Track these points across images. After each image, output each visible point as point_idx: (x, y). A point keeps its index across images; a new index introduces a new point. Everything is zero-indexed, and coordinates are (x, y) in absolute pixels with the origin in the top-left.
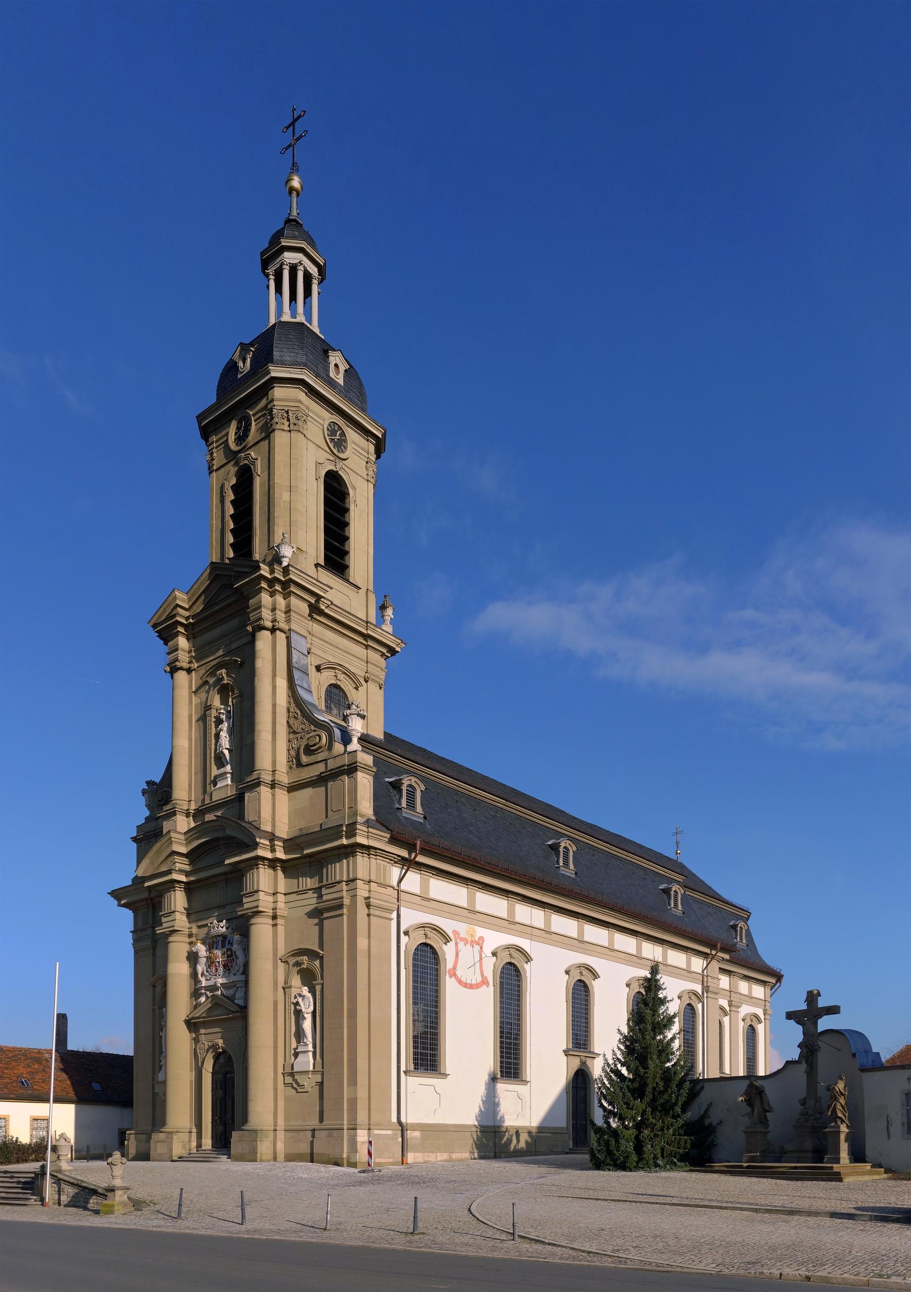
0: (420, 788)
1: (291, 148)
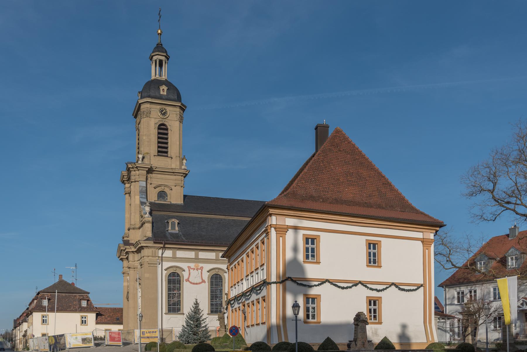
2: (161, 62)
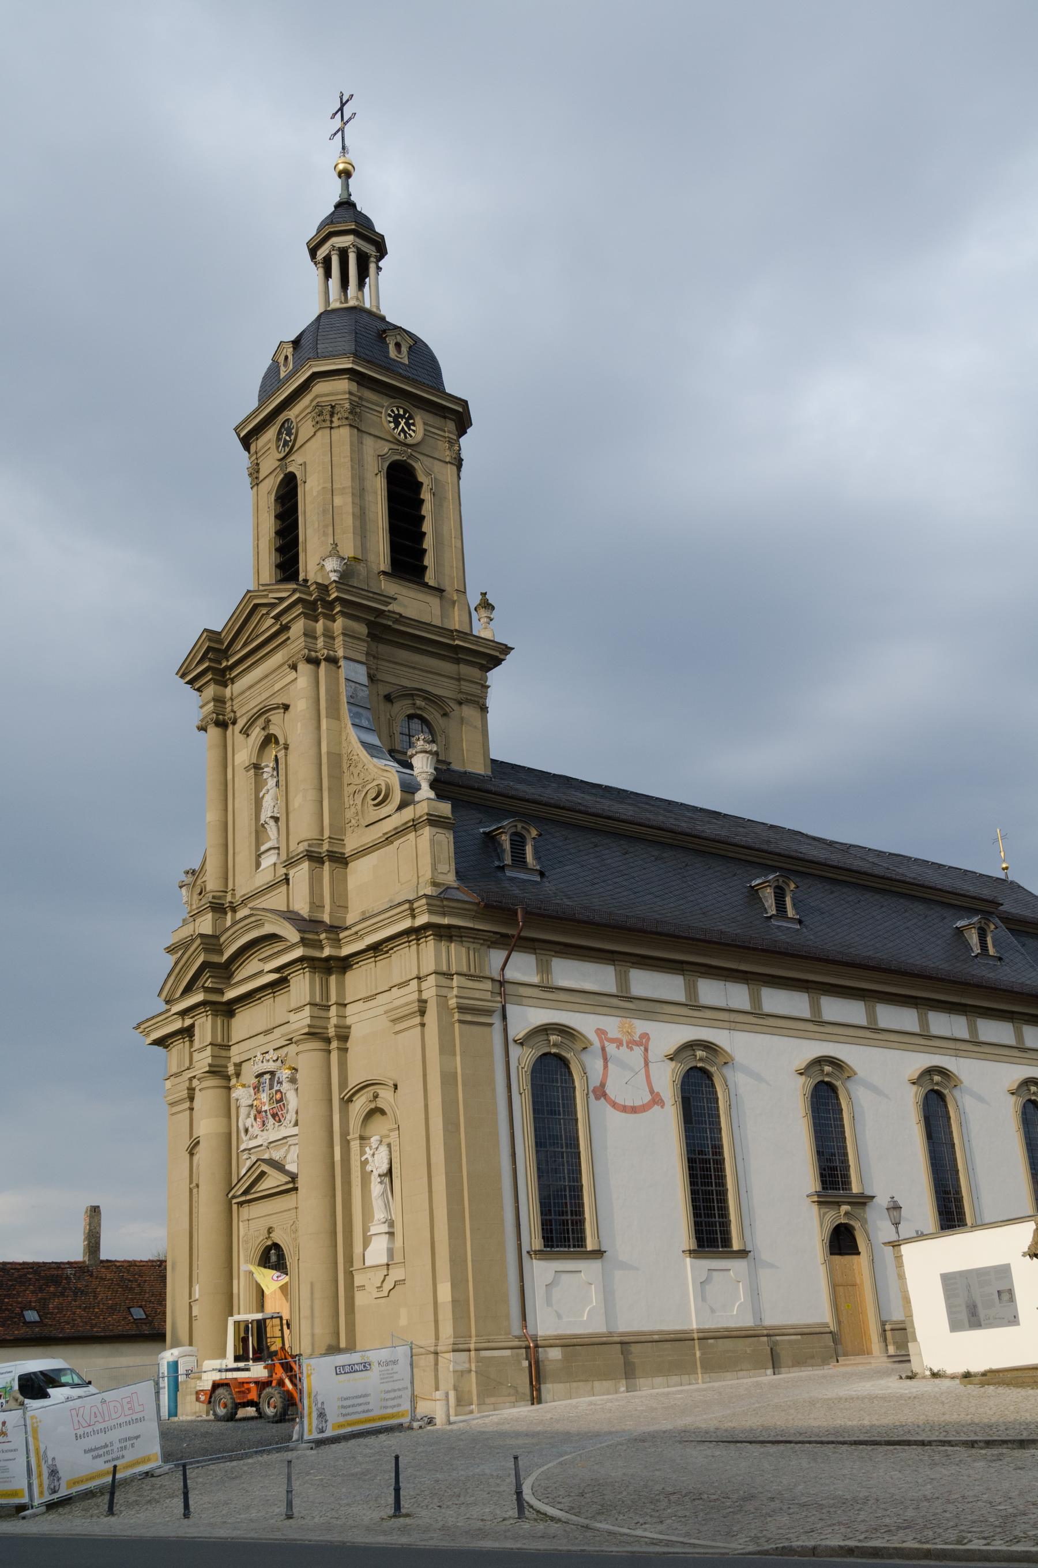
1: (340, 133)
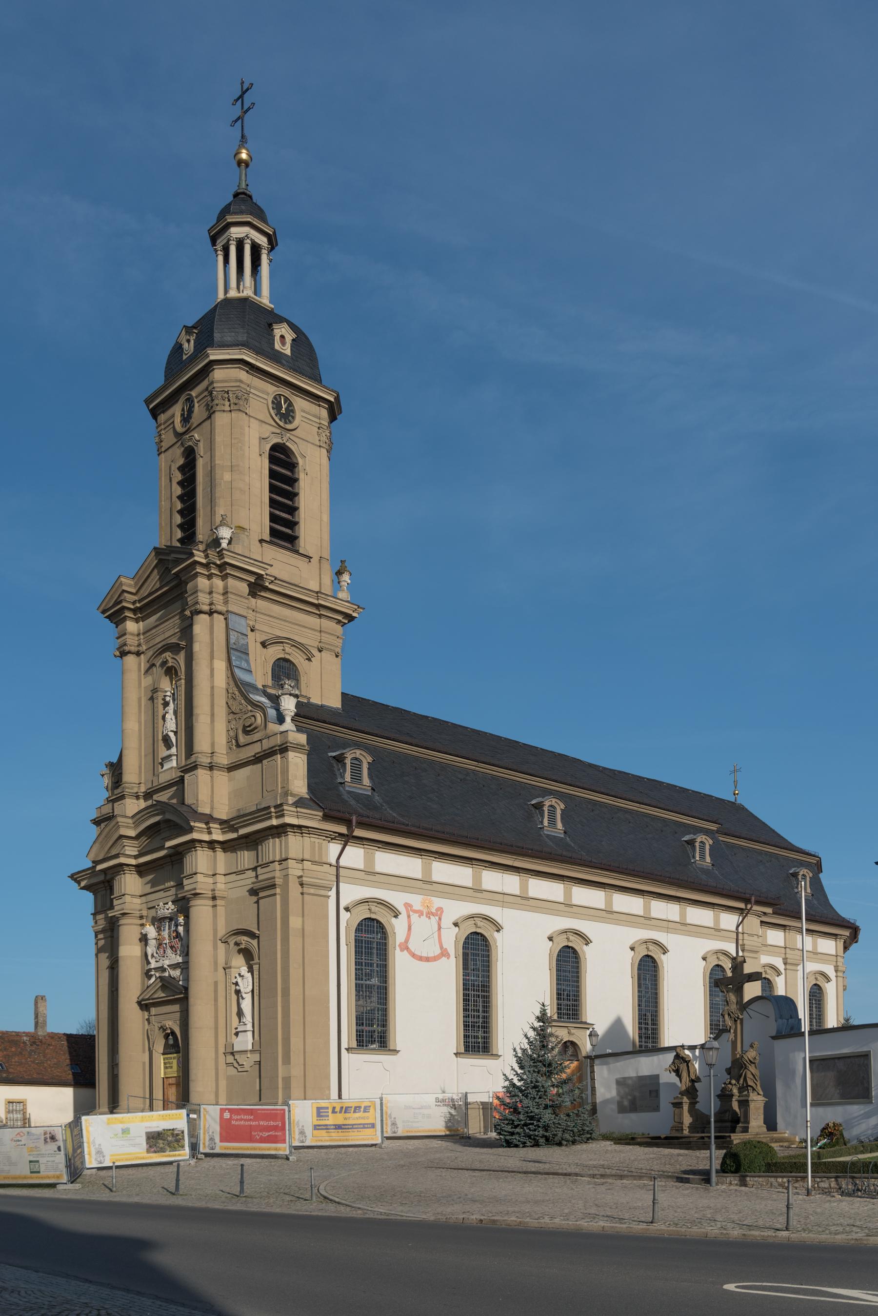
0: (366, 759)
2: (256, 250)
